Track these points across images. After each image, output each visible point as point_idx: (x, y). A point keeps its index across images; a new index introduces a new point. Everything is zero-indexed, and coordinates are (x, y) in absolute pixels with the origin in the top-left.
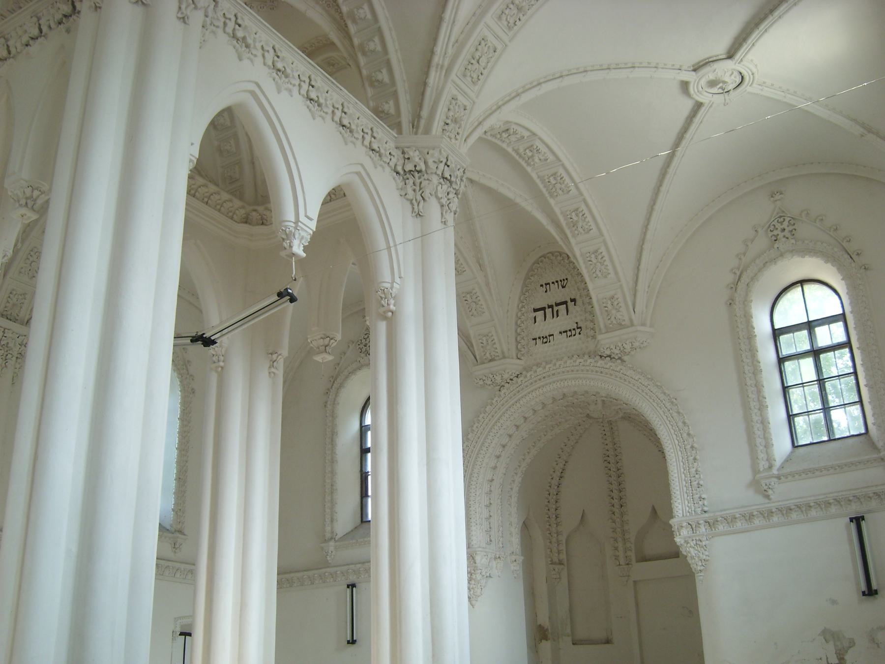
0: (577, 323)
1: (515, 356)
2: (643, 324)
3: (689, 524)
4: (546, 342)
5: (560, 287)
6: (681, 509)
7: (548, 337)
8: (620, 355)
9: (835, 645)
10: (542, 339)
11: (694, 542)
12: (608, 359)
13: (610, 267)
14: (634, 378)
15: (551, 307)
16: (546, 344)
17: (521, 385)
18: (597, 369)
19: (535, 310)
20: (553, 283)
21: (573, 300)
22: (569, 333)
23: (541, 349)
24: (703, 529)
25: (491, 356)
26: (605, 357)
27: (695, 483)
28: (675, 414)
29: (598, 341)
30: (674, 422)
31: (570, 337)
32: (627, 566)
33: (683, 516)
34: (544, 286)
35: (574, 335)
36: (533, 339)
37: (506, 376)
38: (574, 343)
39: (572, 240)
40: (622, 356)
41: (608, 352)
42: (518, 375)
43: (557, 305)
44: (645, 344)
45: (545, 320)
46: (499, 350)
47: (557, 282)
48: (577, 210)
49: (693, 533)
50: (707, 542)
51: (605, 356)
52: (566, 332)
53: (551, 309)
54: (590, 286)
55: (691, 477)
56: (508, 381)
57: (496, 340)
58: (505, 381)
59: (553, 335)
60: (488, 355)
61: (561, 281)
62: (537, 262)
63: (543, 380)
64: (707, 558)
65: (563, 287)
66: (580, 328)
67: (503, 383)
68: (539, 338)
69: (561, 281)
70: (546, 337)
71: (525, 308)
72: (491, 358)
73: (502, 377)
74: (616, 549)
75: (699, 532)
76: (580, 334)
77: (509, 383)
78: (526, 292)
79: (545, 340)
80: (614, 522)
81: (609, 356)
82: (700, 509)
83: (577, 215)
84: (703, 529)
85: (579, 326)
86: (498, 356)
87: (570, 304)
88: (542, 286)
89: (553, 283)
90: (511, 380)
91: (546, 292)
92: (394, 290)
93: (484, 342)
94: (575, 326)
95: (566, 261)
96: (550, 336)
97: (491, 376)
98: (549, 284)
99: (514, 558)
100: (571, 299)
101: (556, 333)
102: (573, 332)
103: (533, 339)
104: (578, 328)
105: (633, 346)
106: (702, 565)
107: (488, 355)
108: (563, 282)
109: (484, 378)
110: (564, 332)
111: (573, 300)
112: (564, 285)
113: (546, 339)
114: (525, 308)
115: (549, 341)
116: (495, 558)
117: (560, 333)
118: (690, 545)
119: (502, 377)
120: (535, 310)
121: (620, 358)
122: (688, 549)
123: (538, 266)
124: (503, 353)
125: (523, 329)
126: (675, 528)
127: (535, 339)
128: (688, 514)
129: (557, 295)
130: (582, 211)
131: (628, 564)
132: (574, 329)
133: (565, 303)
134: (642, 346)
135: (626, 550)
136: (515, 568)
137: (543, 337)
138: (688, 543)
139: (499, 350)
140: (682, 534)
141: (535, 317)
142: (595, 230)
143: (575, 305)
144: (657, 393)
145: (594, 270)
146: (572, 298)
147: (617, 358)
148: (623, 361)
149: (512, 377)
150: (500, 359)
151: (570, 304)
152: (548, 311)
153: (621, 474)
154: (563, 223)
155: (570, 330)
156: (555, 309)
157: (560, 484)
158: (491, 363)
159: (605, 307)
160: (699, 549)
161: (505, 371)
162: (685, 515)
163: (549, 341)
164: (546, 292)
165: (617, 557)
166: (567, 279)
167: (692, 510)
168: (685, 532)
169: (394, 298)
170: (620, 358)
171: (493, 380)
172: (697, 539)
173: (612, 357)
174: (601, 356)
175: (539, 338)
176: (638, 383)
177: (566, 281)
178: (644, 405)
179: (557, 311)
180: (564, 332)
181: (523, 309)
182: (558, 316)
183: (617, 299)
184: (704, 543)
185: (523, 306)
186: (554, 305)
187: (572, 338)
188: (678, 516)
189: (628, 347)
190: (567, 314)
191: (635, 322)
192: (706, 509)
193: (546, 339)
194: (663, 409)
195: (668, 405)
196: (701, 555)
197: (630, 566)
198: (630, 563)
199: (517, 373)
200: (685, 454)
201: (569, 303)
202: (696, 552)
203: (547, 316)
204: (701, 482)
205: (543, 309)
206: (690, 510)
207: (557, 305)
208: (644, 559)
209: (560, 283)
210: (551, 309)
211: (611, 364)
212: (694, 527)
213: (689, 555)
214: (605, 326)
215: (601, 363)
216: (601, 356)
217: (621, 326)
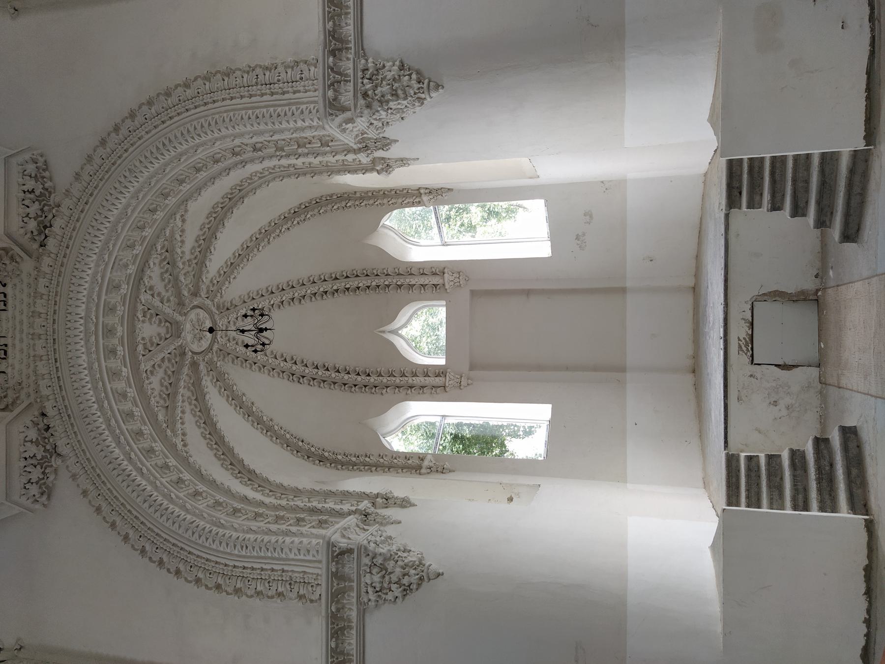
3: (332, 84)
18: (61, 256)
24: (347, 66)
31: (5, 305)
37: (33, 434)
50: (370, 60)
55: (257, 84)
64: (397, 63)
73: (31, 441)
84: (347, 66)
105: (33, 175)
106: (410, 75)
119: (31, 441)
149: (41, 426)
171: (34, 461)
184: (370, 65)
189: (30, 184)
215: (51, 243)
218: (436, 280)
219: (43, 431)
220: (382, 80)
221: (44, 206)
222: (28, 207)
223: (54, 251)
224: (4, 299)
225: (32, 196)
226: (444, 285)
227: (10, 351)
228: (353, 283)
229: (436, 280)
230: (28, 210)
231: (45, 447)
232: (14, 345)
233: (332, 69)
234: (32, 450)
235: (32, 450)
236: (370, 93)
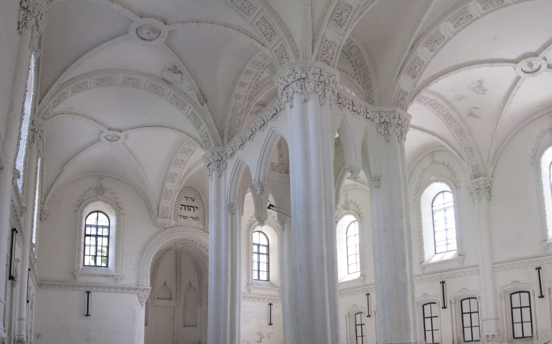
4: (184, 219)
9: (260, 337)
15: (188, 206)
19: (182, 205)
20: (189, 198)
21: (197, 207)
22: (194, 219)
23: (182, 220)
26: (207, 232)
35: (196, 220)
36: (180, 216)
37: (170, 226)
38: (195, 223)
47: (191, 198)
52: (193, 218)
57: (169, 212)
59: (187, 217)
61: (192, 198)
65: (193, 201)
69: (192, 198)
79: (184, 218)
87: (196, 209)
88: (185, 197)
89: (189, 198)
91: (186, 200)
96: (186, 217)
98: (188, 197)
102: (195, 219)
110: (192, 217)
111: (197, 207)
113: (185, 217)
117: (190, 217)
120: (182, 205)
127: (180, 216)
129: (189, 203)
133: (194, 207)
141: (181, 208)
151: (196, 209)
152: (187, 207)
155: (194, 218)
156: (190, 208)
158: (165, 219)
175: (182, 216)
177: (194, 199)
179: (190, 209)
180: (192, 217)
182: (190, 211)
187: (195, 221)
193: (185, 217)
201: (195, 208)
203: (186, 209)
205: (185, 206)
210: (188, 207)
218: (178, 299)
226: (176, 300)
227: (185, 219)
228: (179, 276)
229: (178, 299)
232: (185, 220)
234: (167, 225)
235: (167, 225)
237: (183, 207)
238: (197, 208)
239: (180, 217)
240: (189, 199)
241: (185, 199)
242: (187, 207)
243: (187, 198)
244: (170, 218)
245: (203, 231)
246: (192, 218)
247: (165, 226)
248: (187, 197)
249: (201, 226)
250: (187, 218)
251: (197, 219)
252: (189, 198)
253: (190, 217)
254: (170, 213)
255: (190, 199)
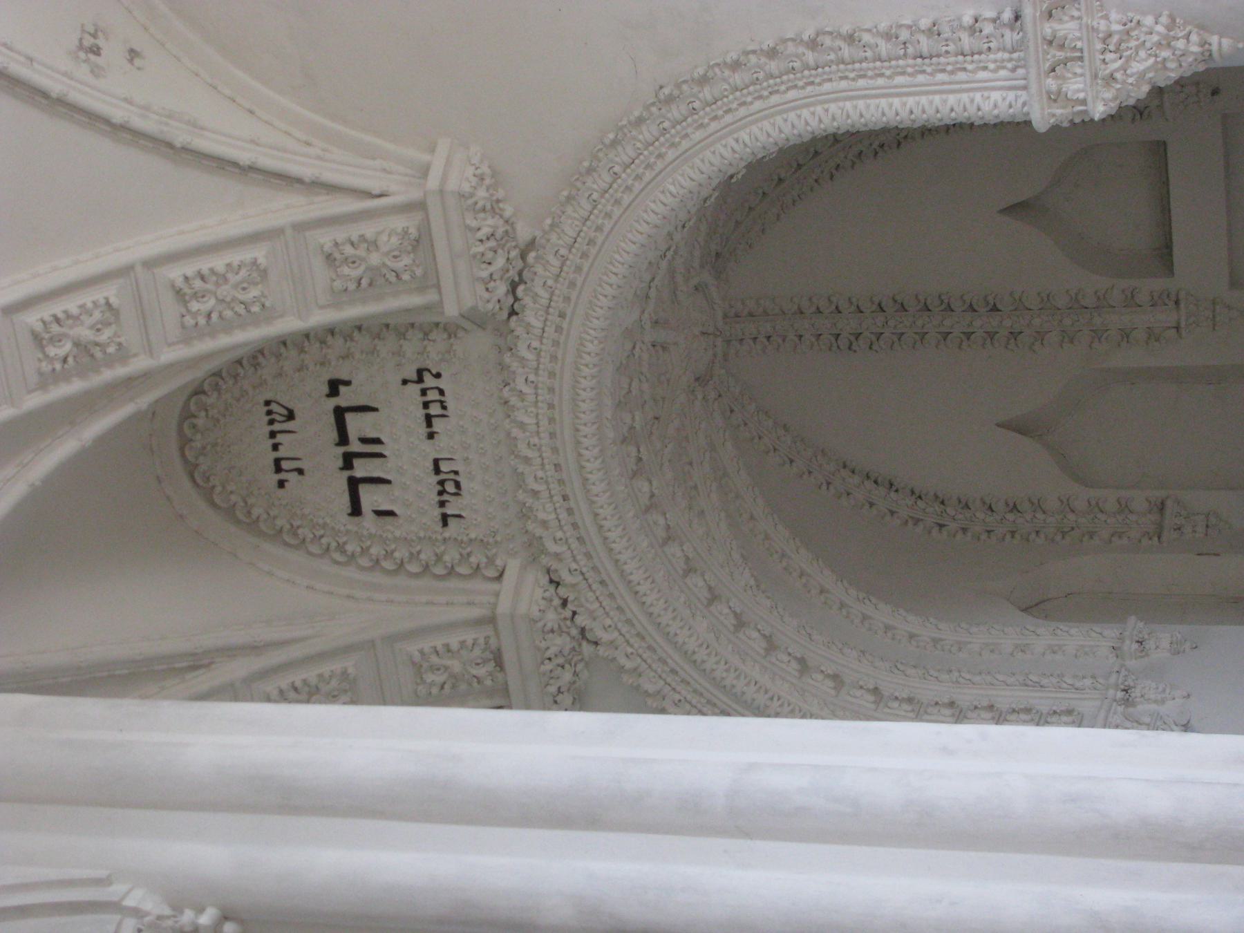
0: (405, 382)
1: (495, 586)
2: (425, 171)
4: (458, 485)
5: (286, 426)
6: (1004, 93)
7: (442, 477)
8: (514, 253)
10: (445, 497)
11: (1109, 56)
12: (520, 290)
13: (235, 257)
14: (586, 214)
15: (348, 460)
16: (463, 485)
17: (583, 574)
18: (550, 330)
19: (356, 510)
20: (275, 447)
21: (334, 387)
22: (435, 410)
25: (485, 661)
26: (516, 299)
27: (925, 44)
28: (707, 93)
29: (463, 316)
30: (731, 97)
31: (444, 408)
32: (1182, 305)
33: (1025, 88)
34: (283, 476)
35: (442, 392)
36: (445, 524)
37: (552, 618)
39: (141, 363)
40: (515, 247)
41: (502, 288)
42: (551, 581)
43: (343, 439)
44: (485, 169)
45: (388, 482)
46: (469, 636)
47: (273, 434)
48: (37, 338)
49: (1081, 59)
51: (511, 300)
52: (429, 419)
53: (356, 462)
54: (289, 324)
55: (905, 55)
56: (568, 614)
58: (568, 623)
59: (436, 462)
60: (481, 672)
61: (271, 422)
62: (208, 495)
63: (572, 504)
65: (291, 416)
66: (420, 373)
67: (574, 632)
68: (442, 504)
69: (271, 422)
70: (442, 483)
71: (345, 543)
72: (492, 664)
73: (552, 631)
74: (1125, 335)
75: (1079, 39)
76: (438, 376)
77: (574, 613)
78: (295, 535)
79: (450, 487)
80: (1041, 336)
81: (513, 287)
82: (1008, 33)
83: (56, 340)
85: (415, 377)
86: (487, 638)
87: (346, 397)
88: (281, 484)
89: (275, 447)
90: (565, 603)
91: (300, 472)
92: (148, 906)
93: (439, 678)
94: (414, 389)
95: (211, 400)
96: (437, 470)
97: (548, 666)
98: (277, 462)
99: (1130, 646)
100: (328, 396)
101: (431, 450)
102: (433, 395)
103: (445, 524)
104: (420, 380)
106: (1187, 37)
107: (481, 672)
108: (278, 418)
109: (552, 689)
110: (429, 424)
111: (334, 387)
112: (285, 412)
114: (345, 543)
115: (452, 476)
116: (1127, 702)
117: (431, 436)
118: (1117, 70)
120: (356, 510)
121: (523, 256)
122: (1130, 80)
123: (219, 489)
124: (478, 622)
125: (411, 554)
126: (1061, 113)
127: (445, 519)
128: (1021, 72)
130: (44, 322)
131: (1177, 303)
132: (424, 392)
133: (340, 413)
134: (488, 181)
135: (1130, 300)
136: (1165, 643)
137: (440, 493)
138: (1112, 76)
139: (469, 636)
140: (1081, 95)
141: (380, 513)
142: (110, 292)
143: (347, 383)
144: (639, 145)
145: (240, 309)
146: (325, 389)
147: (520, 264)
148: (532, 244)
149: (557, 602)
150: (497, 635)
151: (346, 397)
152: (362, 469)
153: (895, 301)
154: (75, 386)
155: (426, 405)
156: (355, 446)
157: (913, 492)
158: (509, 657)
159: (359, 284)
160: (1133, 44)
161: (536, 622)
162: (1022, 82)
163: (452, 476)
164: (300, 472)
165: (1153, 335)
166: (268, 403)
167: (1011, 60)
168: (1075, 86)
169: (178, 909)
170: (523, 256)
171: (561, 660)
172: (1099, 46)
173: (517, 279)
174: (513, 313)
175: (442, 504)
176: (603, 201)
177: (274, 407)
178: (672, 188)
179: (364, 441)
180: (429, 424)
181: (349, 548)
182: (377, 441)
183: (336, 244)
185: (341, 548)
186: (342, 450)
187: (449, 400)
188: (1024, 104)
189: (488, 224)
190: (375, 410)
191: (415, 195)
192: (1007, 15)
194: (689, 130)
195: (675, 112)
196: (1155, 38)
197: (1182, 295)
198: (1173, 297)
199: (544, 580)
200: (834, 67)
202: (1142, 54)
203: (375, 474)
204: (925, 23)
205: (354, 484)
206: (1009, 65)
207: (343, 439)
208: (1164, 253)
209: (276, 427)
211: (538, 282)
212: (1061, 55)
213: (1151, 75)
214: (421, 289)
215: (532, 316)
216: (513, 313)
217: (420, 242)
219: (560, 610)
220: (1137, 48)
221: (509, 253)
222: (490, 263)
223: (537, 324)
224: (438, 397)
225: (492, 243)
230: (492, 269)
231: (568, 634)
233: (1050, 43)
234: (559, 643)
236: (1118, 76)
237: (370, 498)
238: (342, 389)
239: (451, 521)
240: (281, 453)
241: (292, 477)
242: (362, 469)
243: (285, 465)
244: (492, 620)
245: (520, 331)
246: (438, 425)
247: (566, 652)
248: (278, 469)
249: (478, 344)
250: (444, 467)
251: (429, 381)
252: (281, 453)
253: (431, 436)
254: (452, 626)
255: (280, 438)
